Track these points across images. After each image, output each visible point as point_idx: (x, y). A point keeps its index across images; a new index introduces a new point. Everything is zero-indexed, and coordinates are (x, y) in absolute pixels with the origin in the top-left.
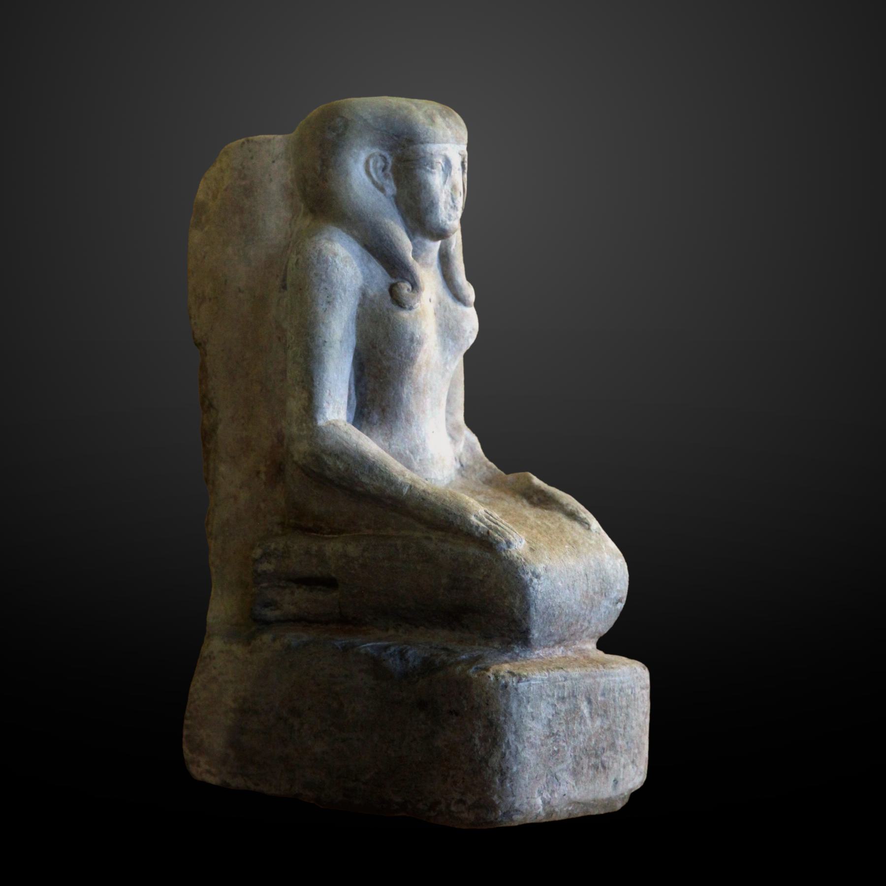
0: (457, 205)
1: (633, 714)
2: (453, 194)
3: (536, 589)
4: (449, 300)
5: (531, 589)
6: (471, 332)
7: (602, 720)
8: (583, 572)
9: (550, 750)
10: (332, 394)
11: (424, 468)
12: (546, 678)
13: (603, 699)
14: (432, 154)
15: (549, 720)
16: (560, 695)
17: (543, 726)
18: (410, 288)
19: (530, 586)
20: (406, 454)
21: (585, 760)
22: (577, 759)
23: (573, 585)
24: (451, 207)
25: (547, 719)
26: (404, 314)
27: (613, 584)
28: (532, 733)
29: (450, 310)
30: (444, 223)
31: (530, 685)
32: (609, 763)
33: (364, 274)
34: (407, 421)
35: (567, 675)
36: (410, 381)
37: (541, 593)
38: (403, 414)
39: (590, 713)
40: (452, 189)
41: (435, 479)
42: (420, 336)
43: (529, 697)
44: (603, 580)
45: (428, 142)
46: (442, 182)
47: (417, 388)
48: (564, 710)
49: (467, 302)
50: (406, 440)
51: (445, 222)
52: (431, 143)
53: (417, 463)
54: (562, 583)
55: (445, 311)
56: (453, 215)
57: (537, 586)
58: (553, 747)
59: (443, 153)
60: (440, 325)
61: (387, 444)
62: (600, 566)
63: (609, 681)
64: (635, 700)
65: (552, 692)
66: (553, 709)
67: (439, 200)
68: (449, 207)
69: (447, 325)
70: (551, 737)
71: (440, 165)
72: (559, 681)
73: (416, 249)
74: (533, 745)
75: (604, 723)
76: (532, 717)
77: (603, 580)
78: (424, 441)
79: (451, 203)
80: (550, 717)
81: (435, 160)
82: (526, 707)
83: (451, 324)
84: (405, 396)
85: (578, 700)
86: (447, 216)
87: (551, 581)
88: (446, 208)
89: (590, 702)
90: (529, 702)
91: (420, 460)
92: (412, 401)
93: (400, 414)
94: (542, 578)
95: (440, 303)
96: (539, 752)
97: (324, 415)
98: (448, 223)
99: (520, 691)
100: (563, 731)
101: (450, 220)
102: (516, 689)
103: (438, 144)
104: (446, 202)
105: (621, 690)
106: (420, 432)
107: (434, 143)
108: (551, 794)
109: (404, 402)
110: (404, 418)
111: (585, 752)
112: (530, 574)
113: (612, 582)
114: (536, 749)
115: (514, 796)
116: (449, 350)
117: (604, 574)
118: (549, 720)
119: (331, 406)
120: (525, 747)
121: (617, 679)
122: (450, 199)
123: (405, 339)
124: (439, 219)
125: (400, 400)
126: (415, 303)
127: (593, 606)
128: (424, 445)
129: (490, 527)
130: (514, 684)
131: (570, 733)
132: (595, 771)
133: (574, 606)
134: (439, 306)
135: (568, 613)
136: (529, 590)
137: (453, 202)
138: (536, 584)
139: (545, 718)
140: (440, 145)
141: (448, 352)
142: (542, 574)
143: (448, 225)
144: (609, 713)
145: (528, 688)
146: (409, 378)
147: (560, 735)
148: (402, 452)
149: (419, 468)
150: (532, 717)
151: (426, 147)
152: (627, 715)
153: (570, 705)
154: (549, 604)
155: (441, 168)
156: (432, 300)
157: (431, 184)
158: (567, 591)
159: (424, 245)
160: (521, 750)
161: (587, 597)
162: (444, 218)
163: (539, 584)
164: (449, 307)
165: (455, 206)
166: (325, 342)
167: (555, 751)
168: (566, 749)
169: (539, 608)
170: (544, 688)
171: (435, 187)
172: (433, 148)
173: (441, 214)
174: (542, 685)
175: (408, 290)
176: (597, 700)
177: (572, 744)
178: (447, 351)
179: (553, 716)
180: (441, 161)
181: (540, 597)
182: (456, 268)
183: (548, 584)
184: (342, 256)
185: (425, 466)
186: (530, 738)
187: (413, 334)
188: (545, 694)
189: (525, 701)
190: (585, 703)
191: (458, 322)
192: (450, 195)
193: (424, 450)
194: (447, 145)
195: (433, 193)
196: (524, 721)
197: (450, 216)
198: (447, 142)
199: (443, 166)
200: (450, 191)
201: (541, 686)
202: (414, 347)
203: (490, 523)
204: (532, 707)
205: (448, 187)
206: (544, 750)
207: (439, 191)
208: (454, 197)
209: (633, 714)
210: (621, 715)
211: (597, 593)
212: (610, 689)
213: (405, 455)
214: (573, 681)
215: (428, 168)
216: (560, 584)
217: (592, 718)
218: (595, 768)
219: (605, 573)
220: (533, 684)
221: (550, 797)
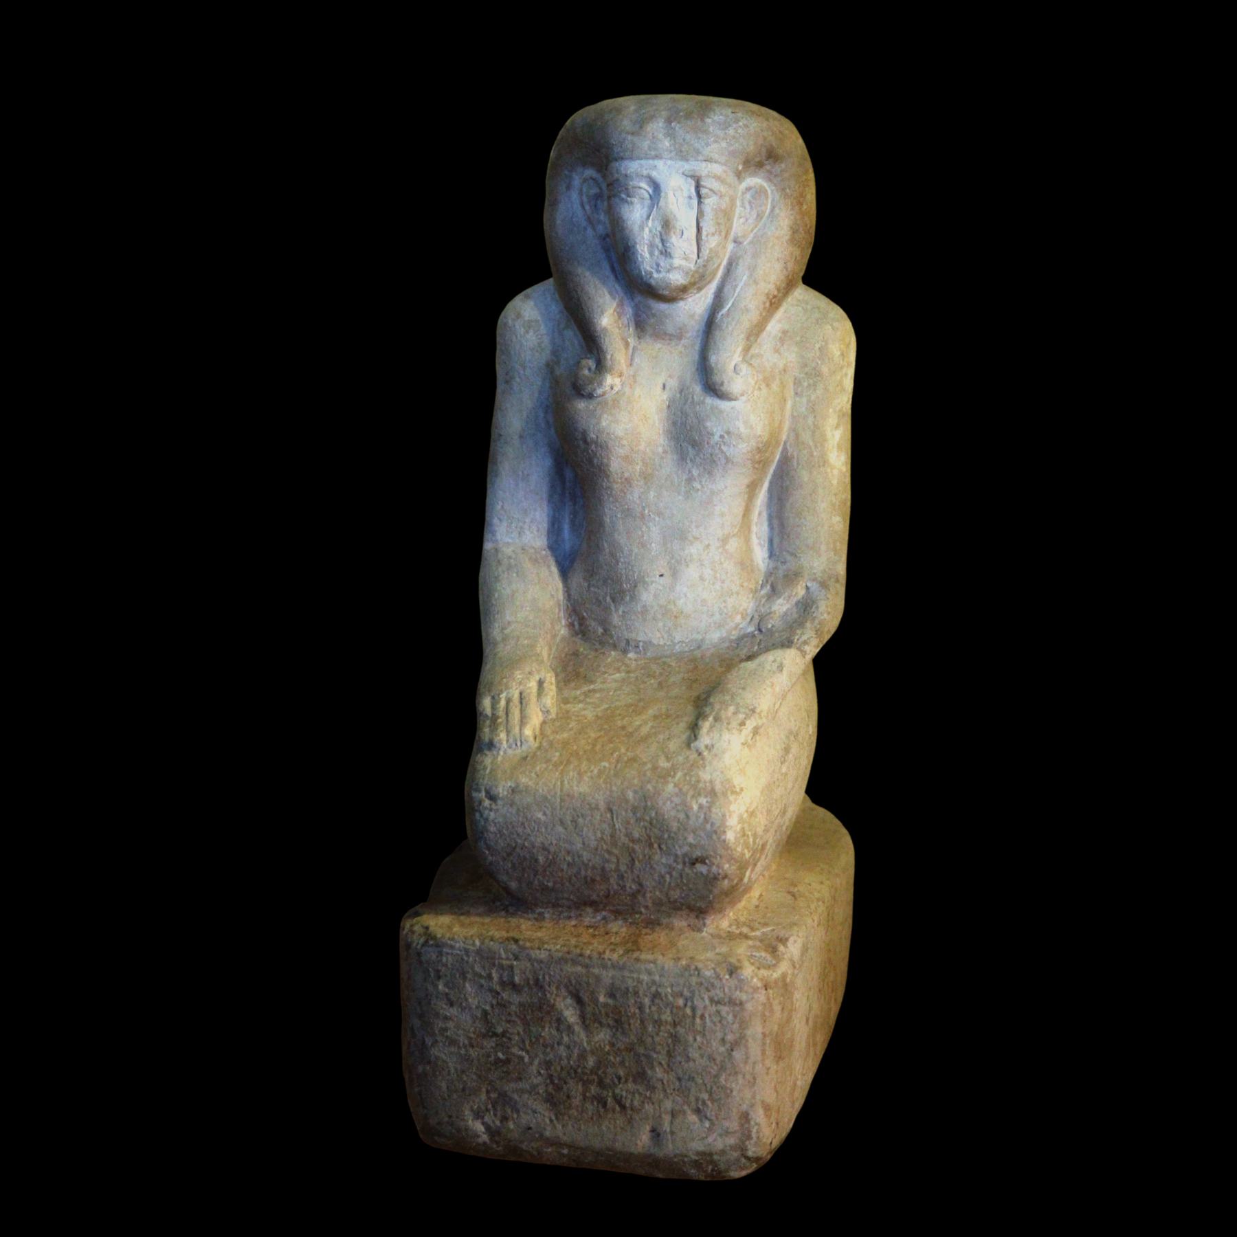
0: (669, 250)
1: (691, 1039)
2: (663, 233)
3: (485, 816)
4: (698, 389)
5: (477, 815)
6: (722, 437)
7: (614, 1034)
8: (602, 806)
9: (489, 1056)
10: (506, 507)
11: (626, 625)
12: (475, 948)
13: (611, 1001)
14: (626, 176)
15: (485, 1013)
16: (505, 979)
17: (474, 1018)
18: (593, 367)
19: (477, 811)
20: (605, 601)
21: (576, 1089)
22: (556, 1081)
23: (574, 821)
24: (661, 253)
25: (480, 1009)
26: (581, 405)
27: (675, 833)
28: (451, 1024)
29: (693, 402)
30: (648, 276)
31: (440, 954)
32: (632, 1101)
33: (554, 344)
34: (613, 555)
35: (520, 952)
36: (611, 499)
37: (495, 823)
38: (606, 545)
39: (583, 1017)
40: (662, 227)
41: (645, 642)
42: (597, 437)
43: (438, 971)
44: (651, 824)
45: (622, 159)
46: (645, 216)
47: (628, 509)
48: (517, 1002)
49: (719, 393)
50: (609, 581)
51: (651, 273)
52: (627, 159)
53: (619, 616)
54: (545, 814)
55: (685, 404)
56: (662, 264)
57: (487, 812)
58: (496, 1052)
59: (645, 173)
60: (674, 423)
61: (586, 584)
62: (646, 802)
63: (623, 977)
64: (694, 1017)
65: (488, 972)
66: (494, 997)
67: (636, 243)
68: (656, 253)
69: (684, 424)
70: (491, 1037)
71: (643, 191)
72: (502, 959)
73: (640, 313)
74: (453, 1042)
75: (617, 1039)
76: (449, 1000)
77: (651, 824)
78: (636, 586)
79: (660, 245)
80: (488, 1008)
81: (631, 183)
82: (436, 986)
83: (690, 421)
84: (607, 520)
85: (547, 993)
86: (655, 267)
87: (518, 810)
88: (651, 254)
89: (579, 1001)
90: (439, 978)
91: (624, 612)
92: (620, 526)
93: (603, 545)
94: (500, 802)
95: (681, 392)
96: (466, 1055)
97: (494, 535)
98: (655, 275)
99: (423, 958)
100: (518, 1034)
101: (658, 272)
102: (419, 954)
103: (638, 161)
104: (652, 246)
105: (656, 995)
106: (631, 573)
107: (631, 159)
108: (501, 1122)
109: (607, 529)
110: (607, 550)
111: (573, 1075)
112: (483, 794)
113: (674, 829)
114: (459, 1048)
115: (424, 1107)
116: (691, 460)
117: (653, 815)
118: (485, 1013)
119: (505, 524)
120: (436, 1041)
121: (645, 977)
122: (658, 241)
123: (576, 439)
124: (640, 271)
125: (601, 524)
126: (595, 390)
127: (633, 860)
128: (634, 591)
129: (494, 718)
130: (419, 947)
131: (534, 1040)
132: (600, 1106)
133: (585, 853)
134: (678, 395)
135: (571, 861)
136: (474, 815)
137: (663, 244)
138: (486, 808)
139: (477, 1007)
140: (643, 162)
141: (690, 464)
142: (501, 795)
143: (654, 279)
144: (626, 1026)
145: (437, 957)
146: (610, 495)
147: (510, 1039)
148: (601, 598)
149: (620, 623)
150: (449, 1000)
151: (620, 165)
152: (675, 1038)
153: (531, 998)
154: (516, 842)
155: (647, 196)
156: (667, 388)
157: (625, 218)
158: (560, 829)
159: (649, 308)
160: (430, 1044)
161: (614, 844)
162: (648, 268)
163: (491, 810)
164: (693, 398)
165: (666, 251)
166: (501, 435)
167: (501, 1061)
168: (526, 1060)
169: (492, 844)
170: (467, 962)
171: (629, 223)
172: (632, 167)
173: (643, 262)
174: (466, 958)
175: (590, 369)
176: (597, 1000)
177: (541, 1056)
178: (688, 462)
179: (492, 1006)
180: (643, 185)
181: (492, 829)
182: (715, 343)
183: (511, 813)
184: (526, 319)
185: (629, 622)
186: (446, 1029)
187: (584, 433)
188: (470, 971)
189: (432, 975)
190: (569, 1001)
191: (700, 420)
192: (658, 234)
193: (633, 598)
194: (660, 163)
195: (627, 232)
196: (432, 1003)
197: (658, 265)
198: (657, 157)
199: (651, 191)
200: (659, 228)
201: (462, 959)
202: (592, 451)
203: (501, 712)
204: (446, 985)
205: (654, 225)
206: (473, 1053)
207: (636, 228)
208: (665, 238)
209: (691, 1039)
210: (658, 1034)
211: (639, 841)
212: (627, 989)
213: (604, 603)
214: (535, 964)
215: (623, 196)
216: (540, 815)
217: (586, 1027)
218: (599, 1102)
219: (656, 813)
220: (448, 954)
221: (498, 1123)
